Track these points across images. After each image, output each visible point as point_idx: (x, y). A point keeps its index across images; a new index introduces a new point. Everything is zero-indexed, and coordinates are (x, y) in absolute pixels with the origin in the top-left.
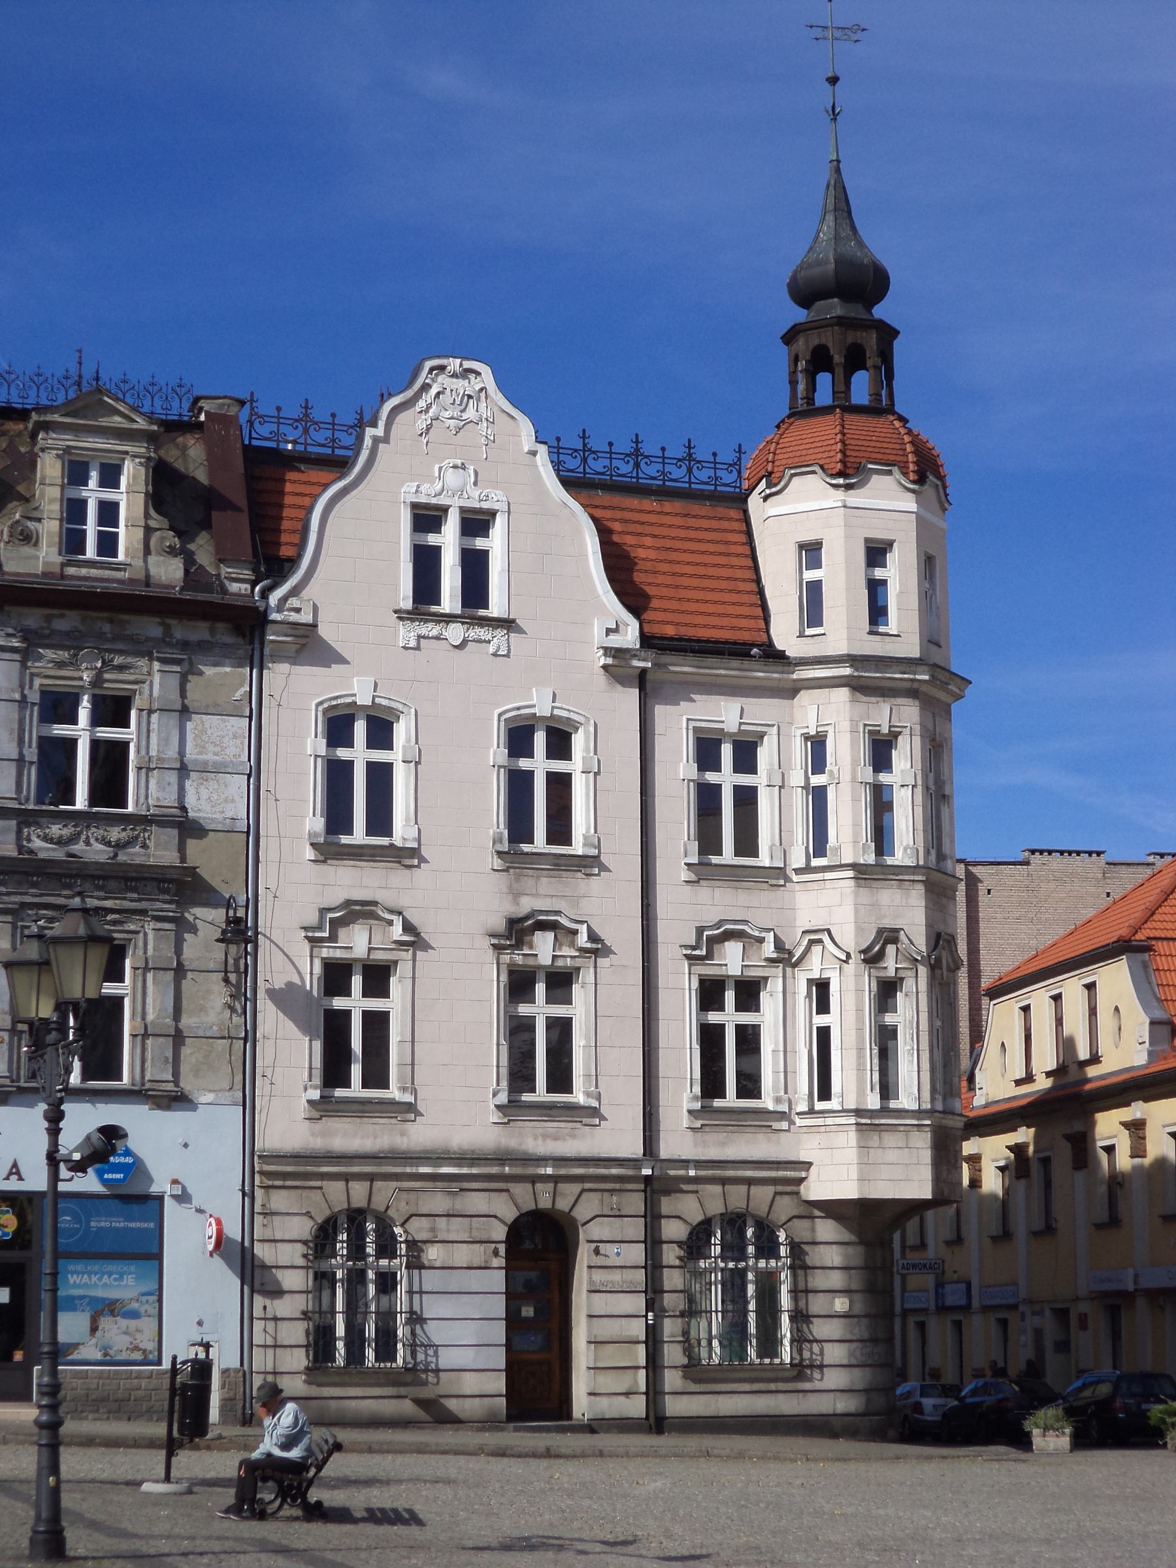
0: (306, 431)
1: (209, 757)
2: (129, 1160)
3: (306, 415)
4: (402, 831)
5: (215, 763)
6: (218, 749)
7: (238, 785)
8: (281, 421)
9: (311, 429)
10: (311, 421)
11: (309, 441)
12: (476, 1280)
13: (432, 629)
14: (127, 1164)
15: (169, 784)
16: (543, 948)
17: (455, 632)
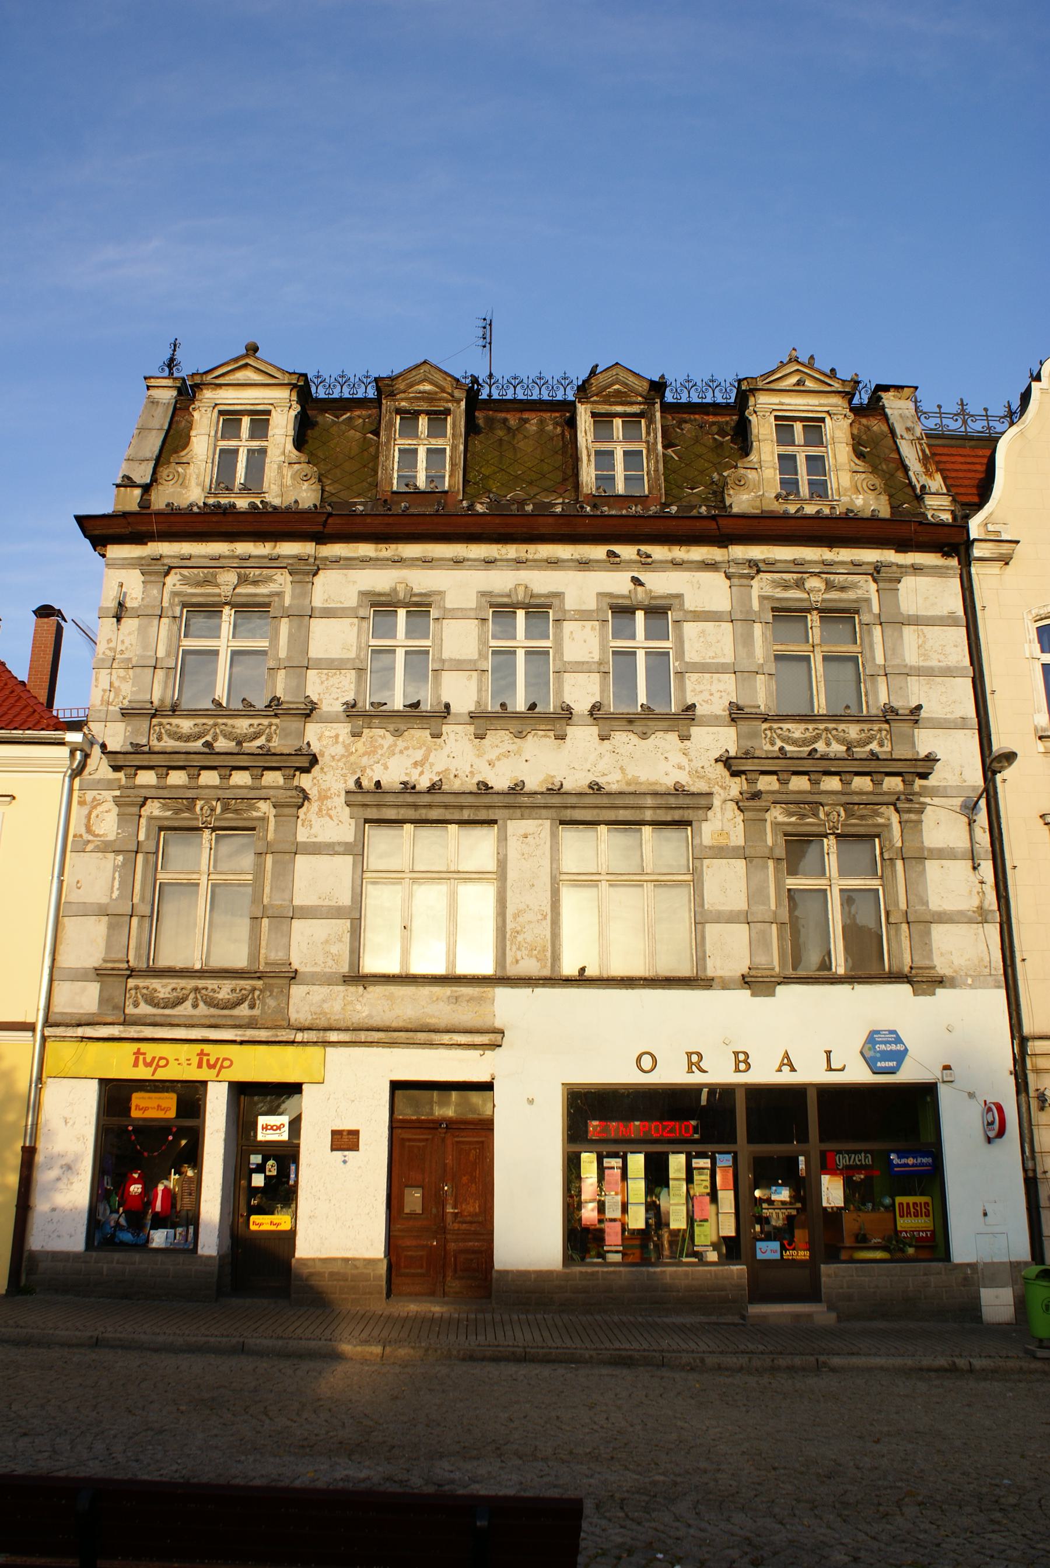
0: (965, 422)
1: (933, 663)
2: (900, 1047)
3: (963, 410)
5: (940, 668)
6: (942, 657)
7: (966, 686)
8: (943, 415)
9: (969, 421)
10: (968, 414)
11: (969, 430)
14: (899, 1051)
15: (901, 688)
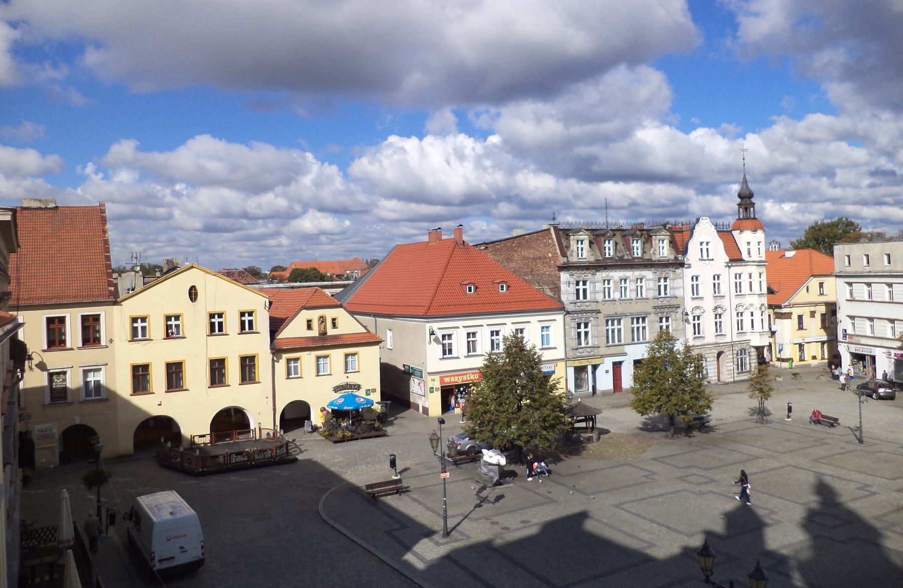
4: (701, 295)
12: (713, 363)
13: (704, 262)
16: (719, 311)
17: (707, 262)
